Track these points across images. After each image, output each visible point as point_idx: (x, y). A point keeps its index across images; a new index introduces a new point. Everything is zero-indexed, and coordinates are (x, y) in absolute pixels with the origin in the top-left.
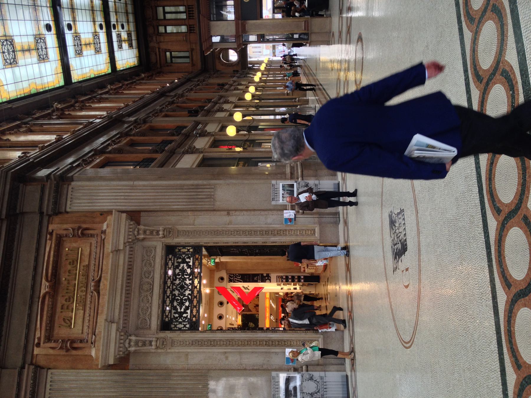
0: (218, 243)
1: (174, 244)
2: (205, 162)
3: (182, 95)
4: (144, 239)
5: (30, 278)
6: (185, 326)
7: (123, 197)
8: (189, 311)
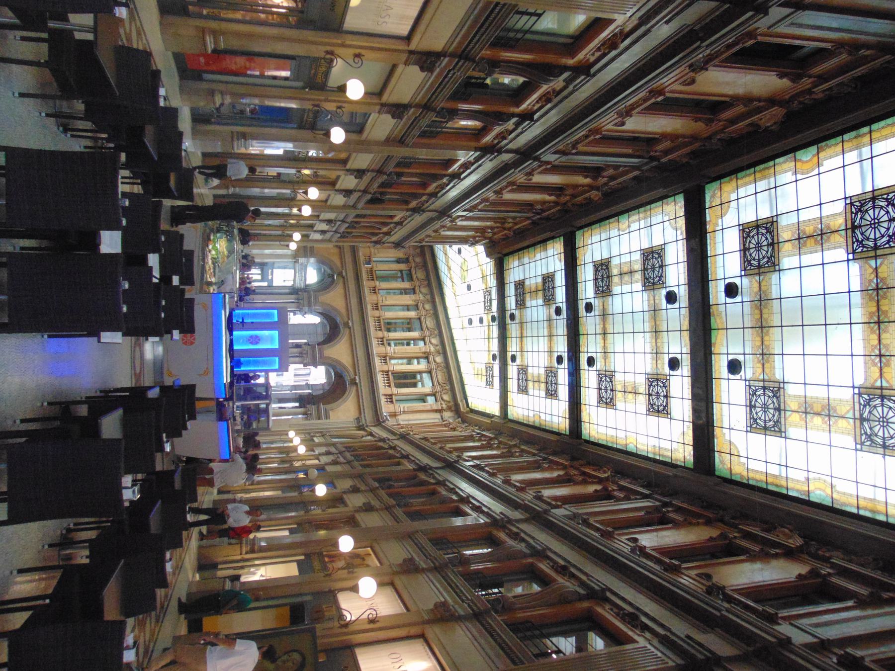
3: (415, 210)
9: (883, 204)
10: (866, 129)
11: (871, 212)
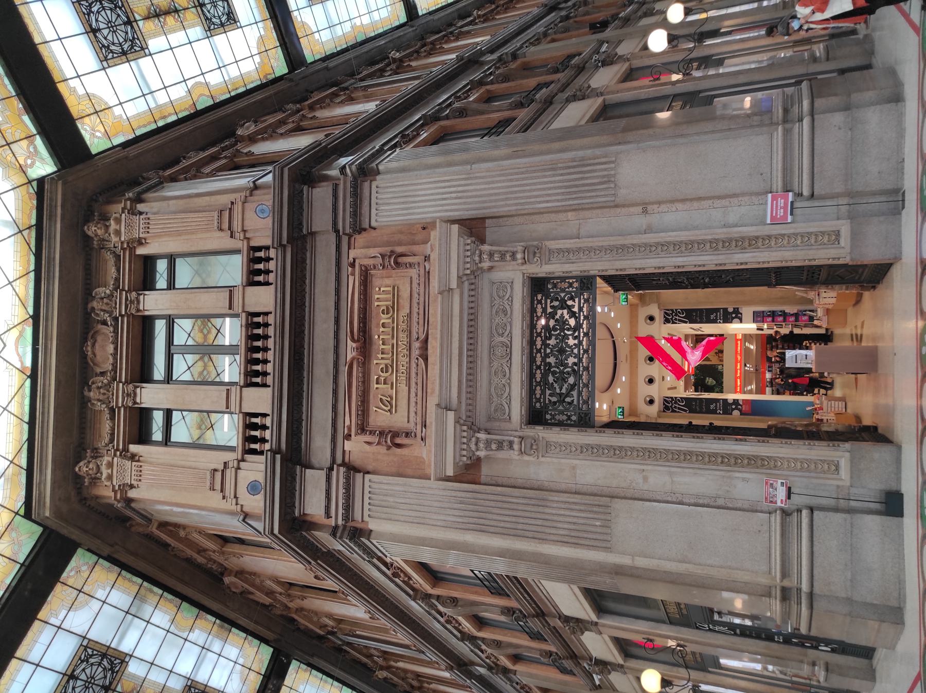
0: (625, 269)
1: (544, 275)
2: (605, 113)
4: (491, 268)
5: (332, 335)
6: (569, 418)
7: (454, 195)
8: (575, 393)
9: (112, 47)
10: (161, 123)
11: (121, 40)
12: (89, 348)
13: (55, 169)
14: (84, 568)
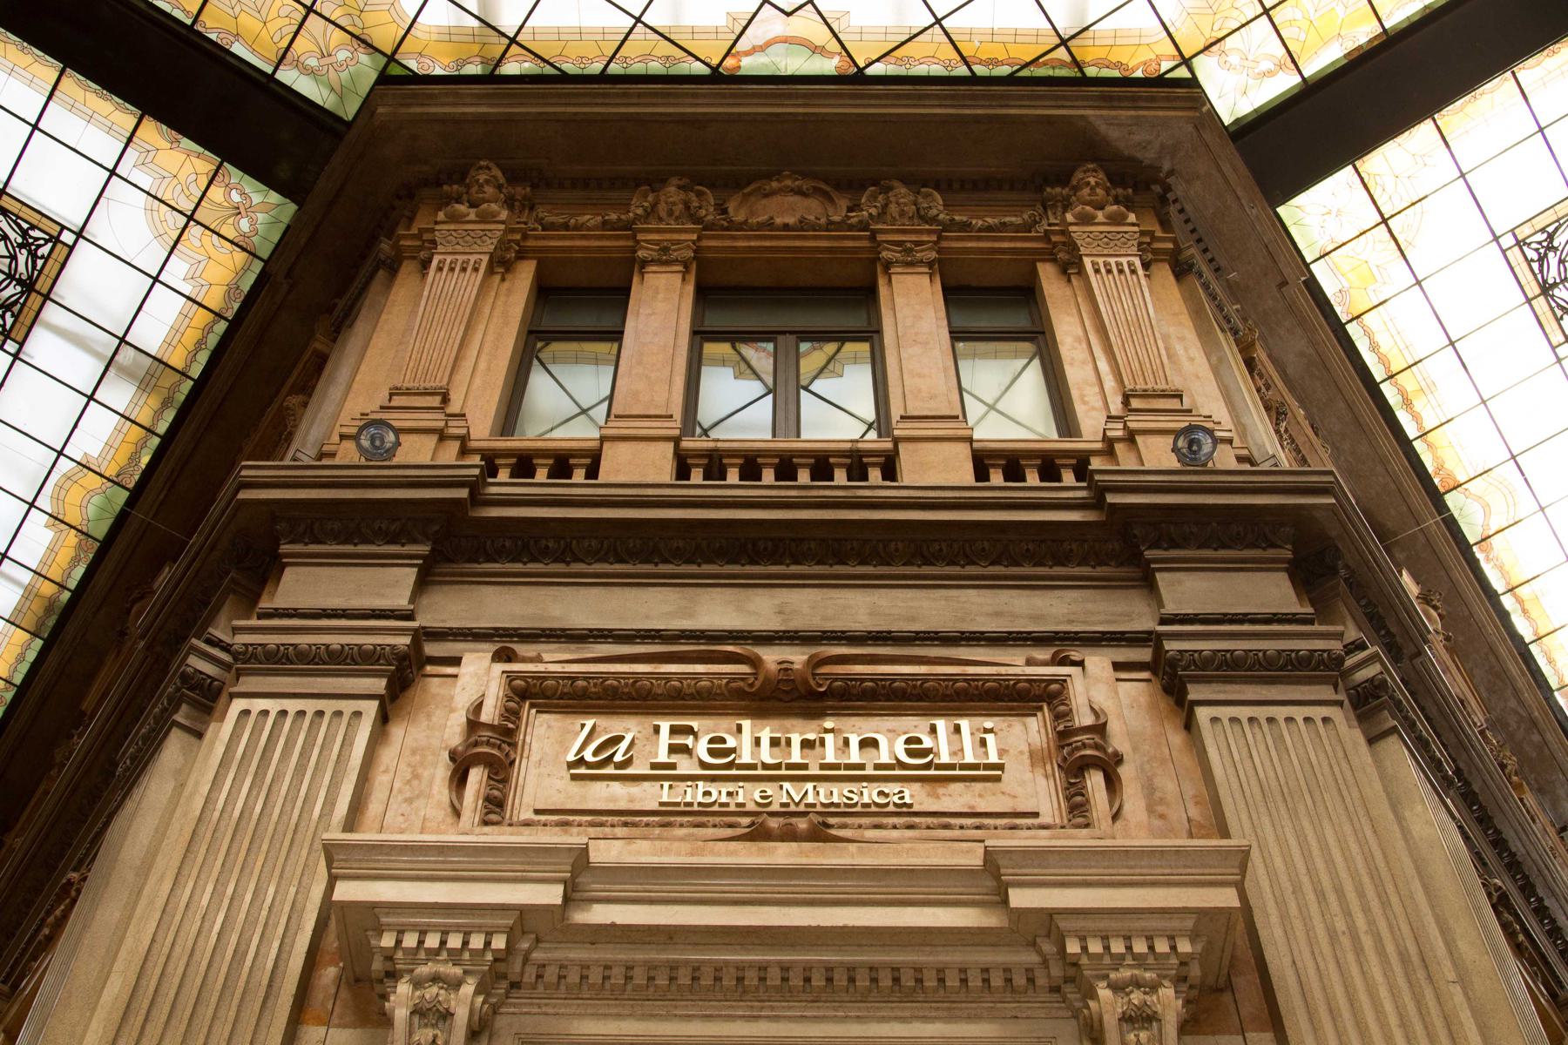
7: (1340, 925)
12: (788, 182)
13: (1227, 121)
14: (245, 225)
